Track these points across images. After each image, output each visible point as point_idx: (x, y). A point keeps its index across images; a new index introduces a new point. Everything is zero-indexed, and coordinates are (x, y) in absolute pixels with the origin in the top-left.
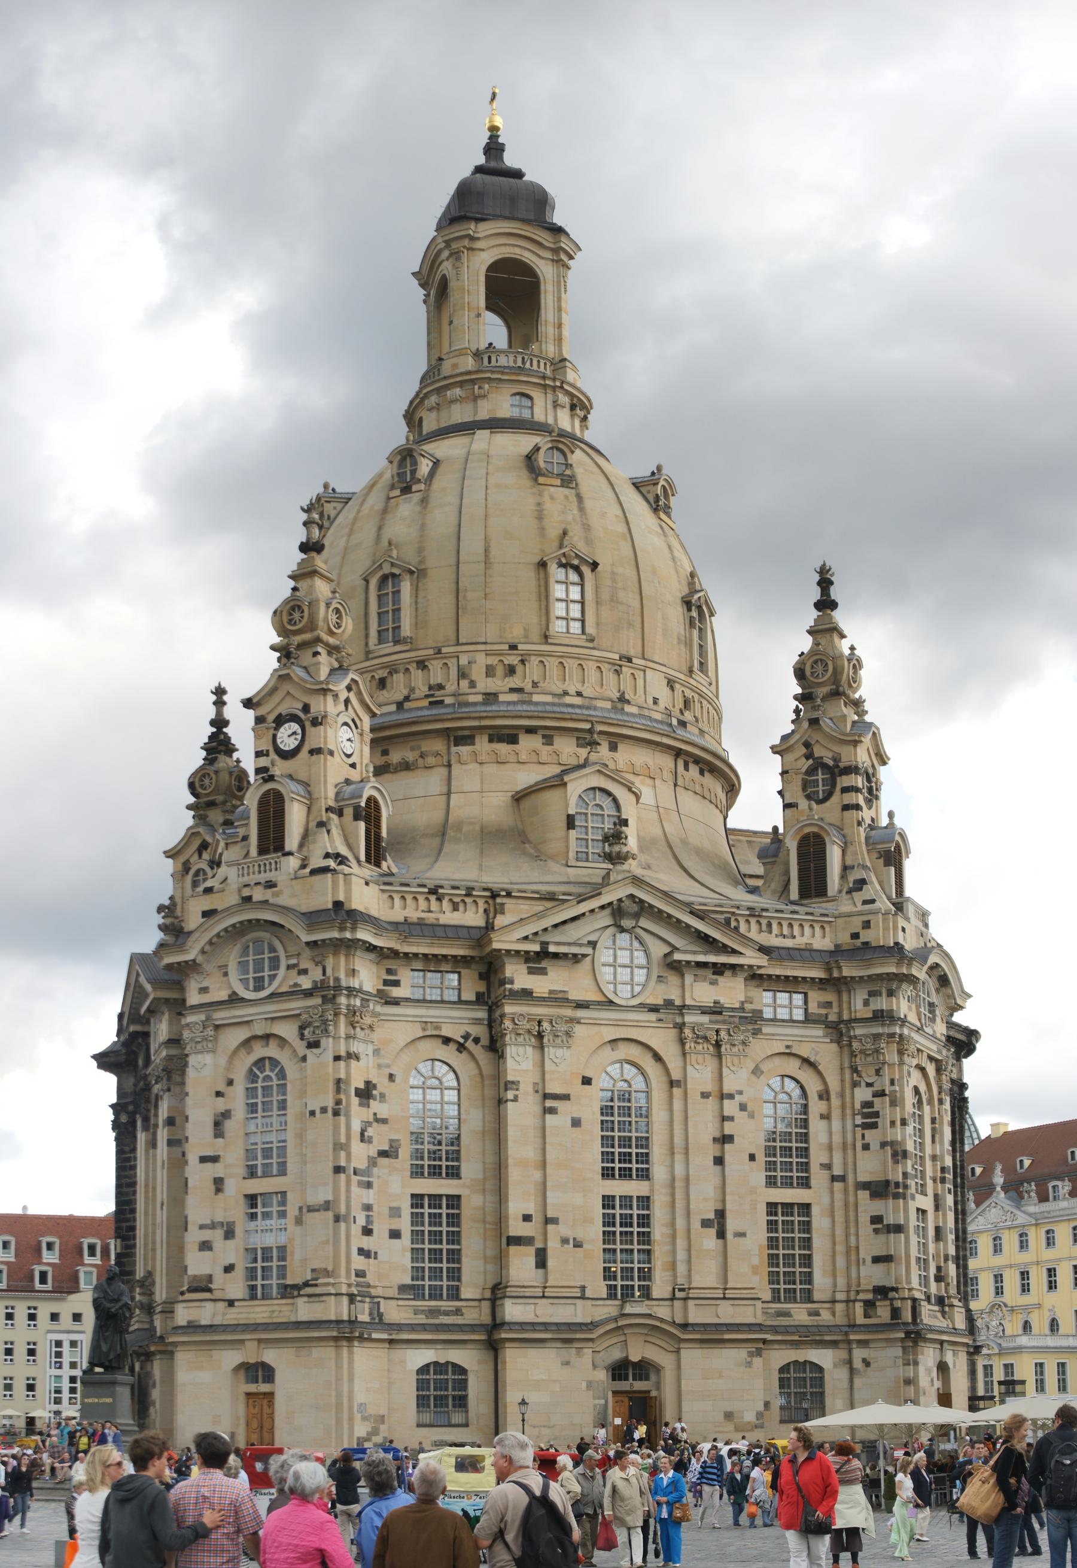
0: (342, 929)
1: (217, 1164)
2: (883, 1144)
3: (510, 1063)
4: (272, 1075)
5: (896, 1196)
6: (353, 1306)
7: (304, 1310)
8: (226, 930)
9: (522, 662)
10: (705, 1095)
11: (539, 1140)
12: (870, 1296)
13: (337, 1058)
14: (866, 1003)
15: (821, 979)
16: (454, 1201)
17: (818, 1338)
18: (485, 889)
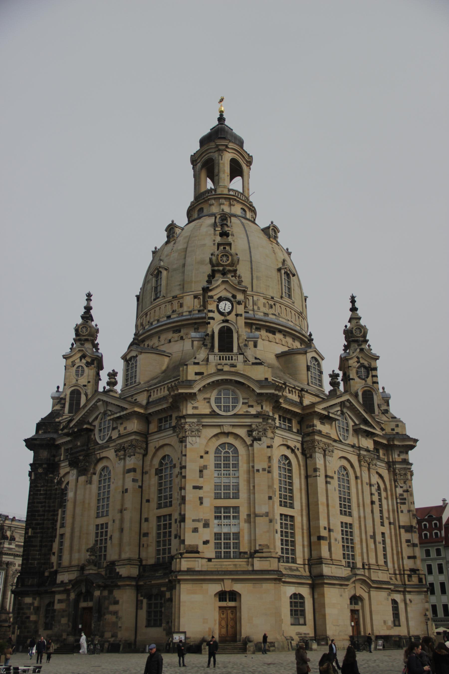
0: (275, 390)
1: (201, 490)
2: (409, 511)
3: (317, 461)
4: (230, 451)
5: (415, 532)
6: (279, 564)
7: (258, 565)
8: (213, 382)
9: (274, 304)
10: (367, 484)
11: (325, 495)
12: (409, 573)
13: (268, 447)
14: (399, 455)
15: (386, 444)
16: (292, 517)
17: (397, 589)
18: (298, 387)
